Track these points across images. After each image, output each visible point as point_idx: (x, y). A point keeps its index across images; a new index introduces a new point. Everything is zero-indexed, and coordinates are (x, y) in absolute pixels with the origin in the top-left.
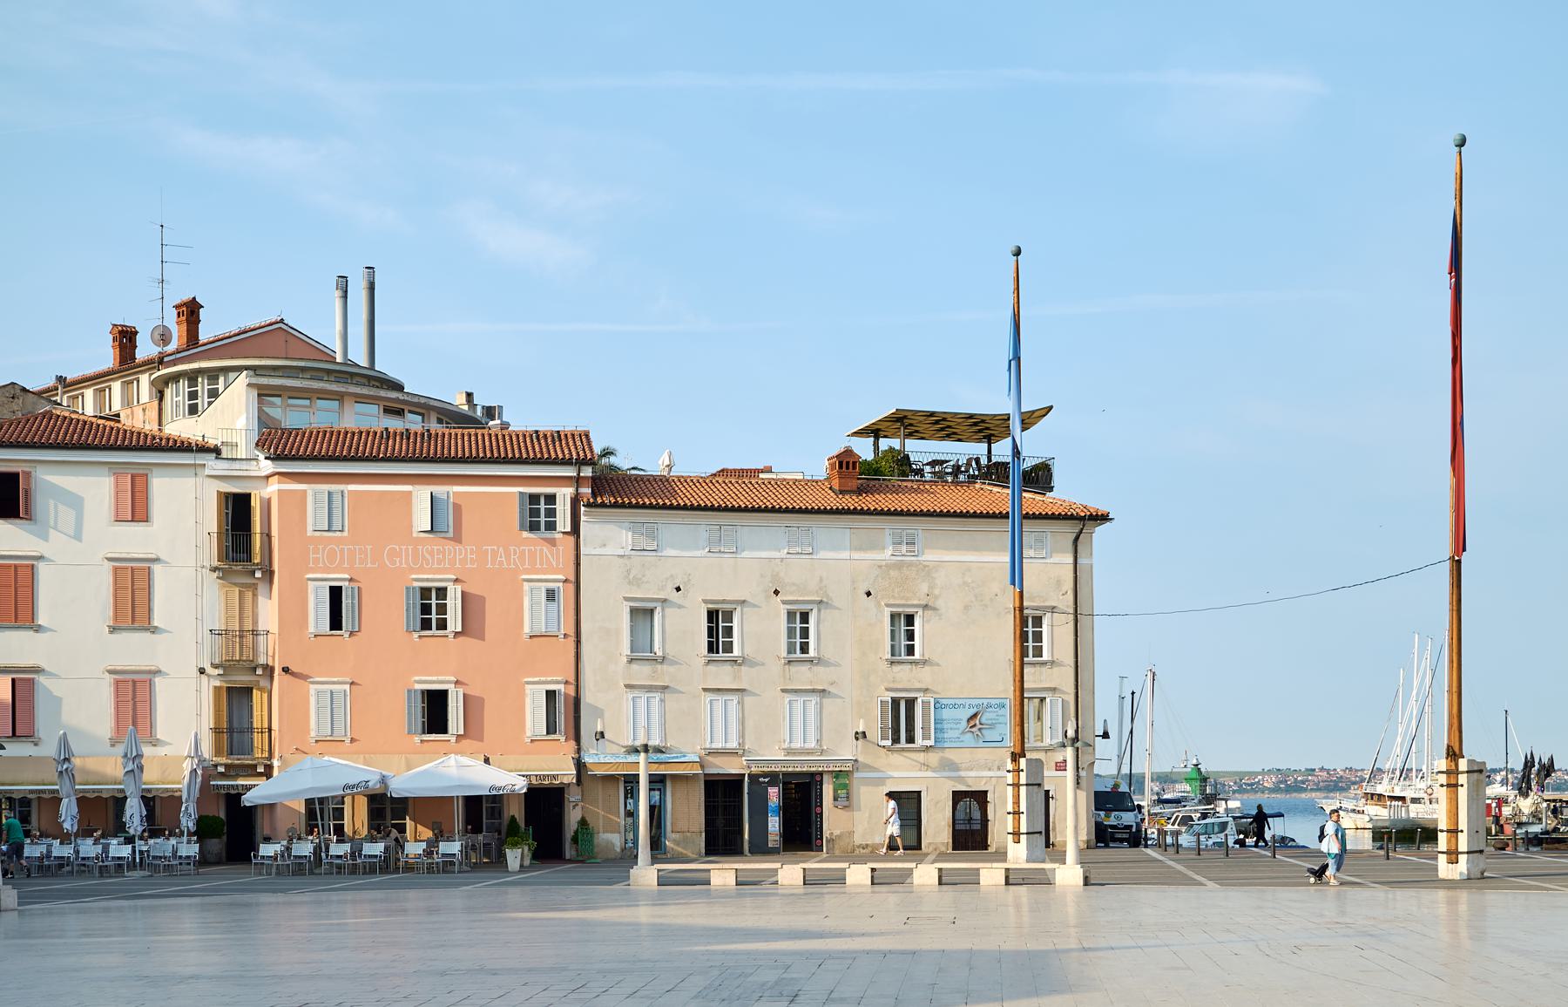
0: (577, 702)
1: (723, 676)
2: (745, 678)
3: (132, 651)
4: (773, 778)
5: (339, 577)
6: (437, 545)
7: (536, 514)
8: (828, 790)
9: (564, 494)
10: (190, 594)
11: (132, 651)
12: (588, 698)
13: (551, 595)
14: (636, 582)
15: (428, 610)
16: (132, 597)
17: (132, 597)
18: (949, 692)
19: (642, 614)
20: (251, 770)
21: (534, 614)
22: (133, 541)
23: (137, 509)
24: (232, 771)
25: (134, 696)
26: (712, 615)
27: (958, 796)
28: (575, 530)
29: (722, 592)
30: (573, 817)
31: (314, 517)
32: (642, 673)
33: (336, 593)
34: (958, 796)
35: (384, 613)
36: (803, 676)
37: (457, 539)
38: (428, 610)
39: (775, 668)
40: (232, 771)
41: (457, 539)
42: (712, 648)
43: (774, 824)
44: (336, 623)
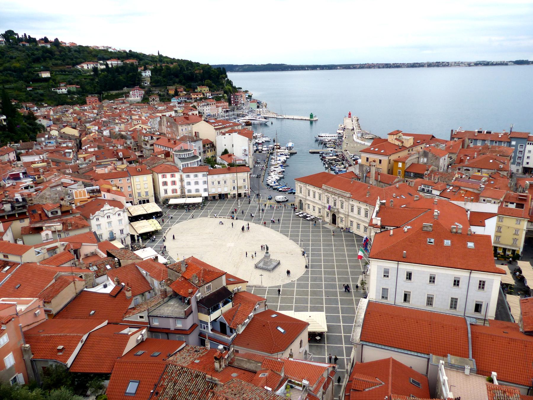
11: (174, 187)
22: (173, 179)
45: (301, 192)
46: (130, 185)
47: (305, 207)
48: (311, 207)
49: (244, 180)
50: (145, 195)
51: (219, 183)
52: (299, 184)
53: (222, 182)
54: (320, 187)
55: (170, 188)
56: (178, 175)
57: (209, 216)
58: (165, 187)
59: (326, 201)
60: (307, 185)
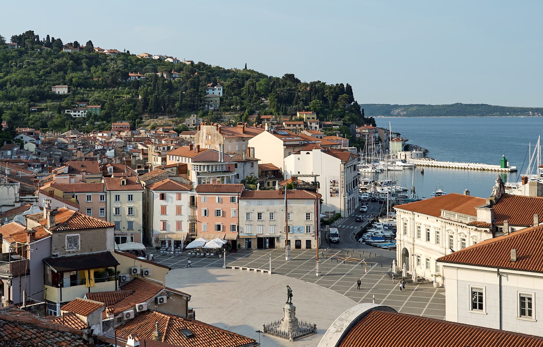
0: (238, 227)
1: (260, 223)
2: (263, 223)
3: (179, 218)
4: (267, 238)
5: (206, 209)
6: (219, 204)
7: (233, 200)
8: (276, 240)
9: (237, 197)
10: (186, 210)
11: (179, 218)
12: (240, 226)
13: (235, 211)
14: (247, 209)
15: (218, 213)
16: (179, 210)
17: (179, 210)
18: (295, 225)
19: (248, 214)
20: (194, 235)
21: (232, 214)
22: (179, 203)
23: (179, 198)
24: (192, 235)
25: (179, 225)
26: (258, 214)
27: (296, 241)
28: (238, 202)
29: (260, 211)
30: (238, 243)
31: (203, 200)
32: (248, 223)
33: (205, 211)
34: (296, 241)
35: (212, 213)
36: (272, 223)
37: (222, 203)
38: (218, 213)
39: (268, 221)
40: (192, 235)
41: (222, 203)
42: (259, 218)
43: (267, 245)
44: (205, 215)
45: (405, 233)
46: (104, 207)
47: (412, 260)
48: (423, 261)
49: (308, 216)
50: (127, 227)
51: (260, 215)
52: (403, 215)
53: (266, 216)
54: (438, 215)
55: (171, 217)
56: (186, 197)
57: (224, 266)
58: (164, 218)
59: (447, 246)
60: (416, 214)
